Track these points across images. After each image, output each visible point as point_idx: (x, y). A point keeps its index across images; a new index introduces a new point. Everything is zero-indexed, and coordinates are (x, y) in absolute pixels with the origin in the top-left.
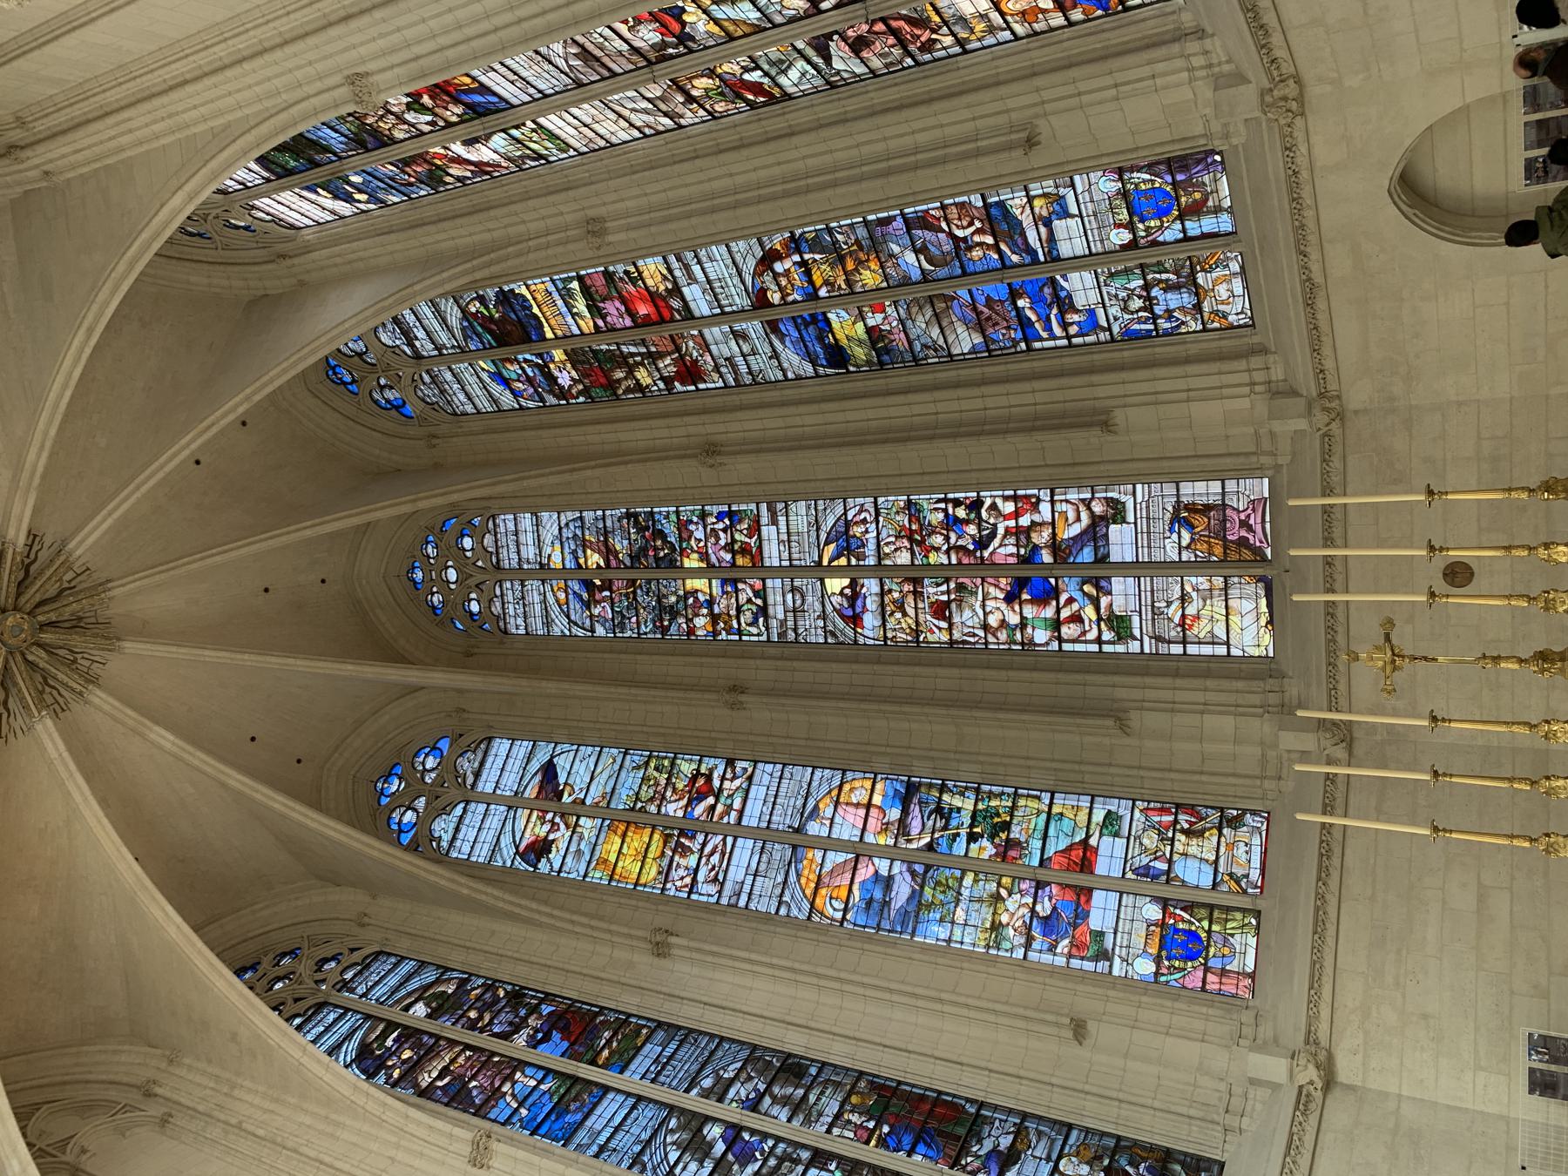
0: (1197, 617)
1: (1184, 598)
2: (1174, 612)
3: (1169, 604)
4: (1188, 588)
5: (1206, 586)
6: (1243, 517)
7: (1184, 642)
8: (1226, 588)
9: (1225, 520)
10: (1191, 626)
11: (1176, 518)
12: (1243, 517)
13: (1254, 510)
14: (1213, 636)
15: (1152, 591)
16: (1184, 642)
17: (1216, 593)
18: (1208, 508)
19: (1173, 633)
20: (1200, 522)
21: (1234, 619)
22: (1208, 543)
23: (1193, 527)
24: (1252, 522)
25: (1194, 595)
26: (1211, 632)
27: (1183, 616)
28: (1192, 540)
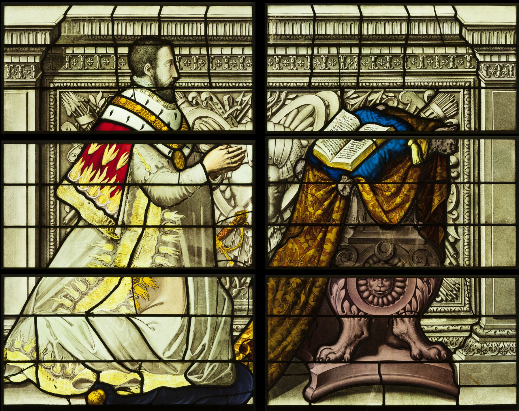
0: (123, 180)
1: (183, 141)
2: (139, 108)
3: (166, 93)
4: (216, 157)
5: (224, 211)
6: (402, 327)
7: (41, 137)
8: (215, 272)
9: (391, 272)
10: (94, 161)
11: (406, 125)
12: (402, 327)
13: (420, 359)
14: (67, 228)
15: (206, 41)
16: (41, 137)
17: (203, 241)
18: (432, 222)
19: (71, 102)
20: (390, 201)
21: (121, 294)
22: (323, 224)
23: (375, 180)
24: (386, 354)
25: (196, 175)
26: (78, 221)
27: (125, 137)
28: (335, 174)
